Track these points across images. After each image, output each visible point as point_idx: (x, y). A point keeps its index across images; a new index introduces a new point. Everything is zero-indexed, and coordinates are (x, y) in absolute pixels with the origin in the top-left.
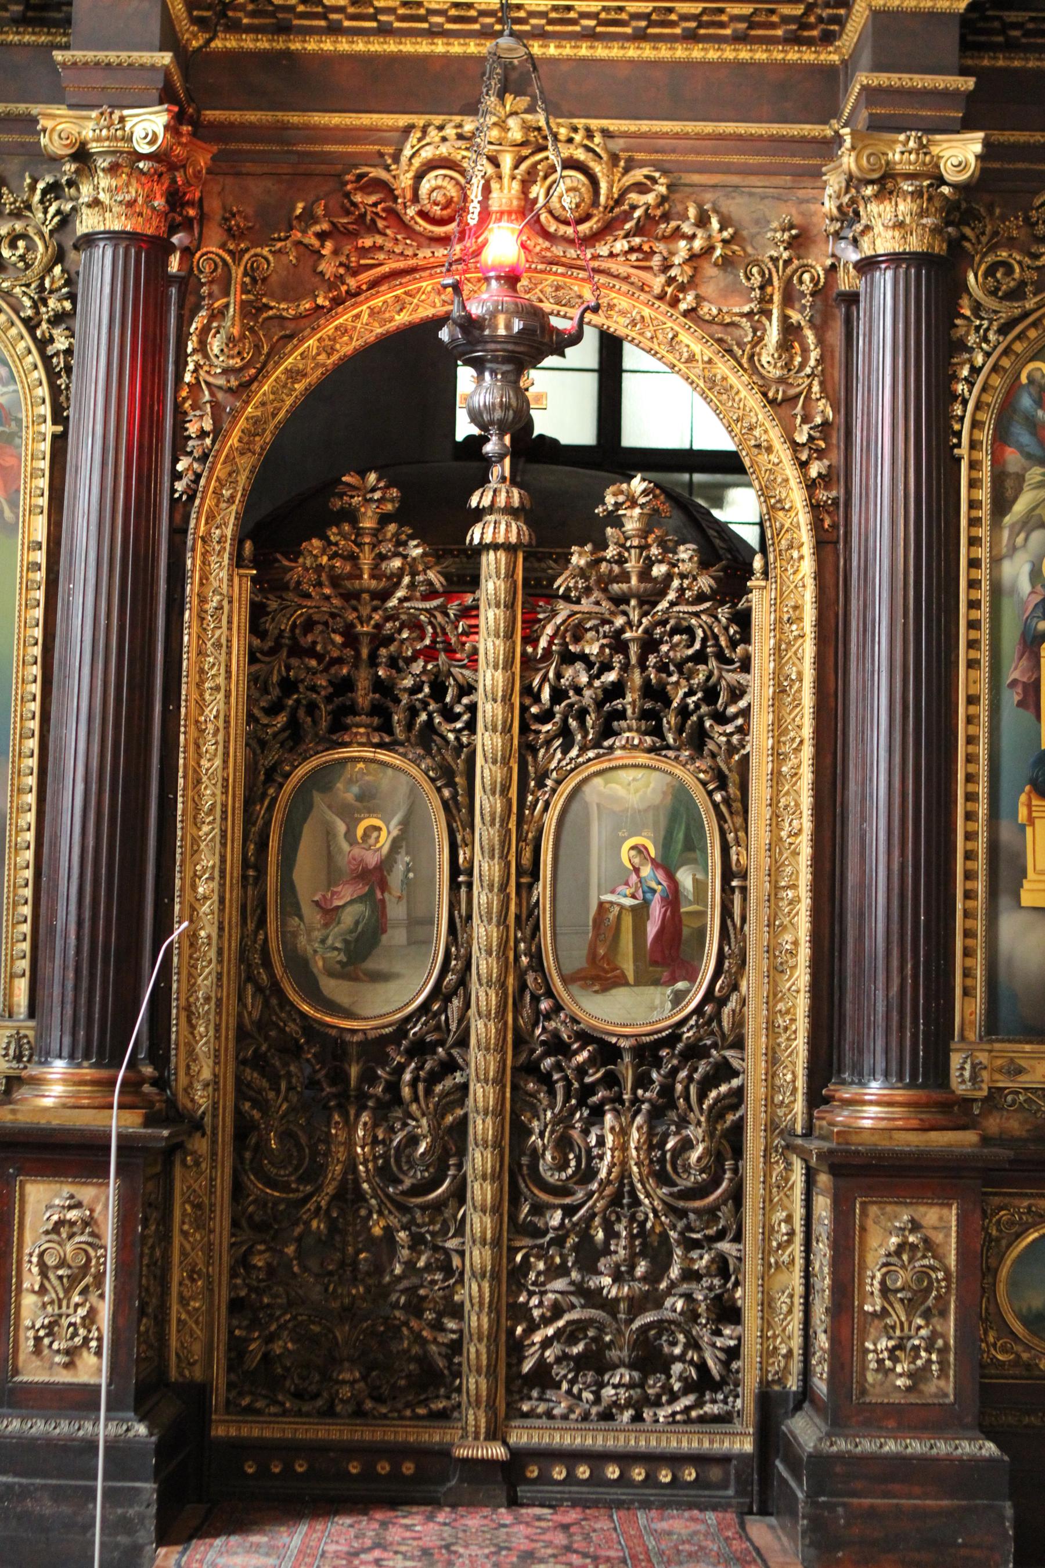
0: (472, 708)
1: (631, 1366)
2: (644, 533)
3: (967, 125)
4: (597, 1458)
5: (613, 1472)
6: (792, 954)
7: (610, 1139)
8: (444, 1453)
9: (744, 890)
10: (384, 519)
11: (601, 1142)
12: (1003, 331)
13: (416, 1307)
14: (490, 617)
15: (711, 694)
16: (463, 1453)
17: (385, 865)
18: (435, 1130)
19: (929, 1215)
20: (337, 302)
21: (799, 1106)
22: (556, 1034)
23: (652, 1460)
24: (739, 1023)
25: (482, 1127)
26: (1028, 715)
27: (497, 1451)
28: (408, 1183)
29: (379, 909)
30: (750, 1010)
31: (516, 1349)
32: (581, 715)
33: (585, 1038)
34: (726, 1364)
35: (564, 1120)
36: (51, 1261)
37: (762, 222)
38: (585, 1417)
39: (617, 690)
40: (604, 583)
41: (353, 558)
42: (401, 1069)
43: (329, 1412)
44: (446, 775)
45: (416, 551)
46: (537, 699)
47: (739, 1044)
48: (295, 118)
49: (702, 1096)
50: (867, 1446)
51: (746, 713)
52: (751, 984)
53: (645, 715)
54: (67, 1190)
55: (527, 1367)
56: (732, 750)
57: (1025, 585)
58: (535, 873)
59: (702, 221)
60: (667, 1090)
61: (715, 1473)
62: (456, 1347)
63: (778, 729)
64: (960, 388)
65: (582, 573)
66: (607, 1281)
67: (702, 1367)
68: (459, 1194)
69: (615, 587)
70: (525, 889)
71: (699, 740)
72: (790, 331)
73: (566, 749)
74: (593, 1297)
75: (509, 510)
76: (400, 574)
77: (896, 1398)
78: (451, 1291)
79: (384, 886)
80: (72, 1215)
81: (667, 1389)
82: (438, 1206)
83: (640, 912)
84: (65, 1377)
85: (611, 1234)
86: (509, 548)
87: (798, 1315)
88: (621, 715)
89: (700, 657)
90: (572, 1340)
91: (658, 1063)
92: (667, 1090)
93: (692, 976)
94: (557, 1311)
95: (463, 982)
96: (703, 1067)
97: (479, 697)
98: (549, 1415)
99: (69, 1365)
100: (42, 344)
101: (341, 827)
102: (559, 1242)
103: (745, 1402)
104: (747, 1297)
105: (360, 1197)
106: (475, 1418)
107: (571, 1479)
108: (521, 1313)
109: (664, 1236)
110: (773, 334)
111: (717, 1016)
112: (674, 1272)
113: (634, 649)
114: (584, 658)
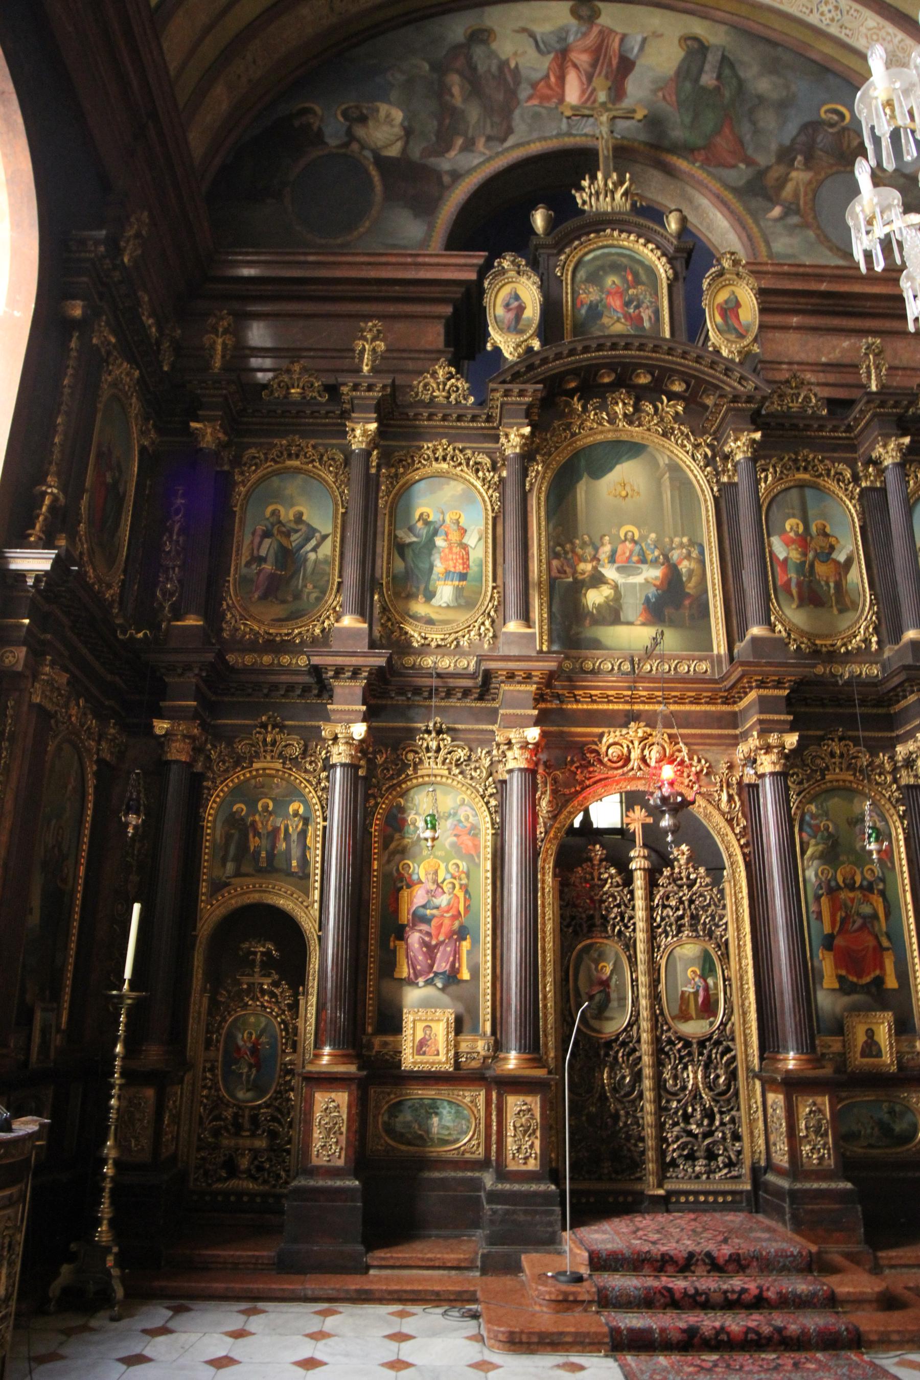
0: (634, 924)
1: (705, 1158)
2: (687, 863)
3: (792, 730)
4: (696, 1193)
5: (702, 1198)
7: (691, 1075)
8: (642, 1193)
9: (730, 985)
12: (798, 795)
13: (628, 1138)
14: (639, 893)
15: (713, 917)
16: (651, 1193)
17: (610, 978)
18: (631, 1074)
19: (819, 1100)
20: (583, 789)
21: (756, 1061)
22: (669, 1038)
23: (716, 1193)
24: (732, 1032)
25: (647, 1072)
26: (819, 922)
27: (661, 1192)
28: (622, 1093)
29: (608, 995)
31: (662, 1153)
32: (671, 925)
33: (680, 1039)
35: (675, 1068)
36: (518, 1125)
37: (718, 761)
38: (690, 1178)
39: (681, 917)
40: (675, 881)
41: (592, 874)
42: (617, 1052)
43: (600, 1179)
44: (627, 947)
45: (613, 871)
46: (655, 920)
47: (733, 1040)
48: (566, 729)
49: (722, 1058)
50: (807, 1186)
51: (726, 924)
53: (691, 925)
54: (522, 1098)
55: (668, 1159)
56: (722, 936)
57: (813, 879)
59: (699, 761)
60: (709, 1057)
61: (738, 1198)
62: (643, 1153)
63: (738, 929)
65: (668, 878)
66: (694, 1127)
67: (729, 1158)
68: (641, 1096)
69: (679, 882)
70: (656, 987)
71: (710, 934)
72: (731, 798)
73: (667, 937)
74: (690, 1133)
75: (644, 857)
77: (814, 1168)
78: (640, 1132)
79: (608, 986)
80: (524, 1108)
81: (718, 1166)
82: (633, 1101)
83: (696, 994)
84: (524, 1168)
85: (694, 1110)
86: (644, 869)
87: (762, 1138)
89: (709, 905)
90: (683, 1150)
91: (705, 1047)
92: (709, 1057)
93: (715, 1015)
95: (637, 1020)
96: (721, 1049)
97: (636, 920)
98: (677, 1177)
99: (525, 1163)
100: (487, 803)
101: (593, 966)
102: (676, 1113)
103: (745, 1170)
105: (607, 1098)
106: (652, 1179)
107: (687, 1202)
108: (665, 1140)
109: (712, 1110)
110: (724, 797)
111: (725, 1029)
112: (717, 1123)
113: (686, 903)
114: (669, 906)
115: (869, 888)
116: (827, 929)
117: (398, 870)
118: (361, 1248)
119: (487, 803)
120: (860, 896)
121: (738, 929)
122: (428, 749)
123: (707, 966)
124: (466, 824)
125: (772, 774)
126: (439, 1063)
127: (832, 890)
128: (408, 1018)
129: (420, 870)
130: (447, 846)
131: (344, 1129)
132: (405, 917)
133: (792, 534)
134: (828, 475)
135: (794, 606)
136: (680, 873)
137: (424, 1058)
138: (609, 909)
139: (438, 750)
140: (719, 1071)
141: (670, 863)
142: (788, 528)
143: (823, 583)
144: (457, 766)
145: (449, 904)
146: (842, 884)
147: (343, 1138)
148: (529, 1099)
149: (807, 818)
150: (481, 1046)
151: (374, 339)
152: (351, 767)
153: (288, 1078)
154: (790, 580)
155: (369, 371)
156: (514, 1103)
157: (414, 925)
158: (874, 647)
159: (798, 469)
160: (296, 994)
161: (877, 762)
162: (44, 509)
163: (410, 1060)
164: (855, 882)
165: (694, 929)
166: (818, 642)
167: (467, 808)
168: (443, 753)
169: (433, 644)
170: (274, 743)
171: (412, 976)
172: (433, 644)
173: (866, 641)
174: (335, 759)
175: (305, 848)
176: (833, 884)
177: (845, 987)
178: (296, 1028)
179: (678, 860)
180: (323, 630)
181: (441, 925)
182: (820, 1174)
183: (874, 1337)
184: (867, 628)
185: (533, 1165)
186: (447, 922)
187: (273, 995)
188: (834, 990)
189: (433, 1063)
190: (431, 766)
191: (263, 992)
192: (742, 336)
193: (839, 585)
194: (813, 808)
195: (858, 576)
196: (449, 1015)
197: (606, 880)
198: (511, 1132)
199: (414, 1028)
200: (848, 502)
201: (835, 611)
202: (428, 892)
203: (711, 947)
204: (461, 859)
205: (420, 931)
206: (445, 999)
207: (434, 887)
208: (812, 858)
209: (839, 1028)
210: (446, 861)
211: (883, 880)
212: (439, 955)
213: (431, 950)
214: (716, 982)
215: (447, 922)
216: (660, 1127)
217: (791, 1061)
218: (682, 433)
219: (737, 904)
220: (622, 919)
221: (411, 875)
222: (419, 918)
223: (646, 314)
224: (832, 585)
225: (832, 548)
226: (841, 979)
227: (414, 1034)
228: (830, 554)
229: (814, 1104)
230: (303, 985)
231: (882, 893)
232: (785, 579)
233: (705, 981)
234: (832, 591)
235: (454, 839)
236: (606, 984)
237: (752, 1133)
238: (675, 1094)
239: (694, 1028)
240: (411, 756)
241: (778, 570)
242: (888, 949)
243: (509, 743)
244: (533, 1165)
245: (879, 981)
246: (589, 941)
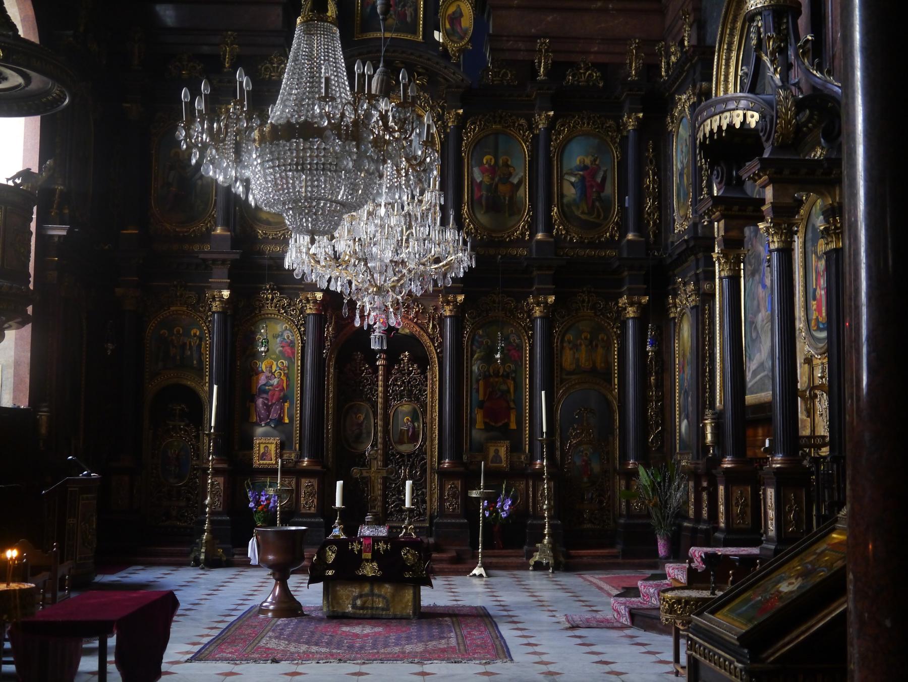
0: (377, 394)
2: (408, 362)
6: (435, 437)
9: (426, 426)
10: (361, 360)
11: (401, 471)
12: (472, 325)
15: (420, 391)
17: (362, 422)
19: (456, 482)
24: (426, 449)
30: (428, 447)
31: (387, 509)
33: (398, 453)
34: (424, 511)
38: (399, 521)
40: (401, 371)
46: (389, 392)
47: (426, 454)
49: (419, 463)
50: (445, 521)
51: (426, 394)
52: (427, 443)
53: (408, 395)
57: (476, 370)
58: (389, 424)
63: (432, 398)
64: (465, 335)
67: (420, 511)
71: (418, 399)
72: (434, 326)
75: (383, 359)
76: (364, 370)
83: (408, 430)
84: (308, 512)
86: (383, 365)
88: (404, 395)
89: (418, 384)
93: (417, 442)
94: (394, 502)
99: (309, 510)
100: (299, 329)
101: (354, 416)
104: (427, 498)
111: (422, 448)
114: (398, 385)
115: (507, 376)
116: (481, 398)
117: (251, 365)
118: (230, 546)
119: (299, 329)
120: (501, 380)
121: (432, 398)
122: (267, 299)
123: (415, 416)
124: (288, 340)
125: (450, 316)
126: (272, 464)
127: (486, 377)
128: (257, 441)
129: (263, 366)
130: (277, 352)
131: (222, 494)
132: (255, 390)
133: (487, 166)
134: (514, 126)
135: (482, 212)
136: (404, 367)
137: (265, 462)
138: (364, 386)
139: (273, 299)
140: (418, 470)
141: (399, 362)
142: (485, 161)
143: (502, 198)
144: (283, 308)
145: (278, 383)
146: (492, 374)
147: (221, 499)
148: (312, 480)
149: (477, 337)
150: (293, 456)
151: (232, 44)
152: (223, 313)
153: (195, 472)
154: (482, 196)
155: (229, 67)
156: (305, 482)
157: (259, 394)
158: (527, 238)
159: (495, 122)
160: (198, 430)
161: (520, 306)
162: (57, 196)
163: (257, 462)
164: (499, 372)
165: (409, 397)
166: (494, 235)
167: (289, 332)
168: (275, 301)
169: (270, 237)
170: (181, 295)
171: (258, 421)
172: (270, 237)
173: (523, 234)
174: (214, 309)
175: (201, 354)
176: (487, 373)
177: (488, 428)
178: (198, 448)
179: (403, 360)
180: (207, 229)
181: (274, 395)
182: (453, 516)
183: (437, 570)
184: (524, 226)
185: (313, 510)
186: (277, 393)
187: (186, 431)
188: (481, 429)
189: (269, 464)
190: (270, 309)
191: (181, 430)
192: (462, 38)
193: (511, 198)
194: (481, 332)
195: (524, 193)
196: (277, 440)
197: (364, 370)
198: (303, 495)
199: (259, 447)
200: (524, 144)
201: (507, 215)
202: (267, 377)
203: (417, 407)
204: (285, 360)
205: (263, 398)
206: (276, 432)
207: (270, 375)
208: (477, 359)
209: (481, 449)
210: (277, 360)
211: (515, 372)
212: (273, 410)
213: (268, 408)
214: (419, 425)
215: (277, 393)
216: (385, 496)
217: (446, 464)
218: (425, 97)
219: (433, 384)
220: (371, 391)
221: (258, 368)
222: (262, 391)
223: (409, 11)
224: (507, 198)
225: (510, 174)
226: (485, 423)
227: (259, 450)
228: (509, 178)
229: (453, 484)
230: (202, 426)
231: (514, 379)
232: (479, 195)
233: (413, 424)
234: (507, 202)
235: (281, 348)
236: (360, 425)
237: (431, 500)
238: (394, 480)
239: (405, 448)
240: (257, 303)
241: (476, 189)
242: (513, 408)
243: (308, 301)
244: (313, 510)
245: (507, 425)
246: (353, 403)
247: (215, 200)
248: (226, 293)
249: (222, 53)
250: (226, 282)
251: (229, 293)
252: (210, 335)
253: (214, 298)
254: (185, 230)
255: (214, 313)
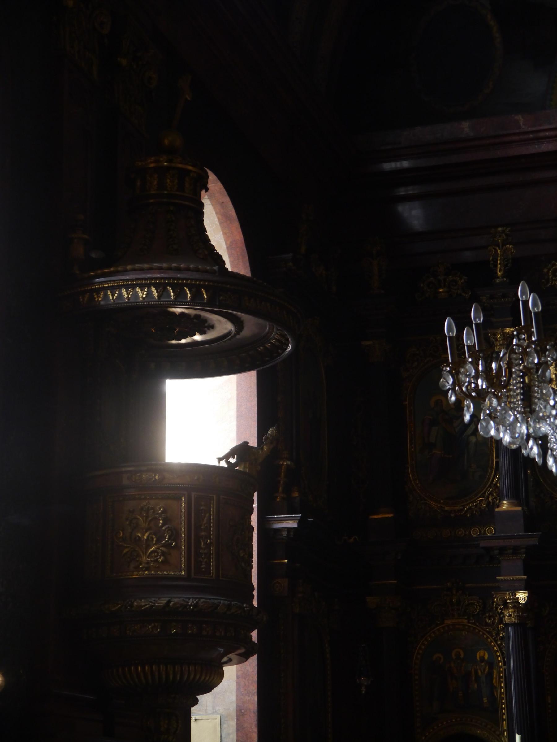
151: (504, 245)
152: (520, 626)
155: (503, 276)
162: (282, 475)
174: (507, 620)
180: (488, 504)
247: (497, 463)
248: (522, 596)
249: (491, 258)
250: (522, 579)
251: (527, 595)
252: (504, 659)
253: (505, 604)
254: (458, 508)
255: (507, 625)
